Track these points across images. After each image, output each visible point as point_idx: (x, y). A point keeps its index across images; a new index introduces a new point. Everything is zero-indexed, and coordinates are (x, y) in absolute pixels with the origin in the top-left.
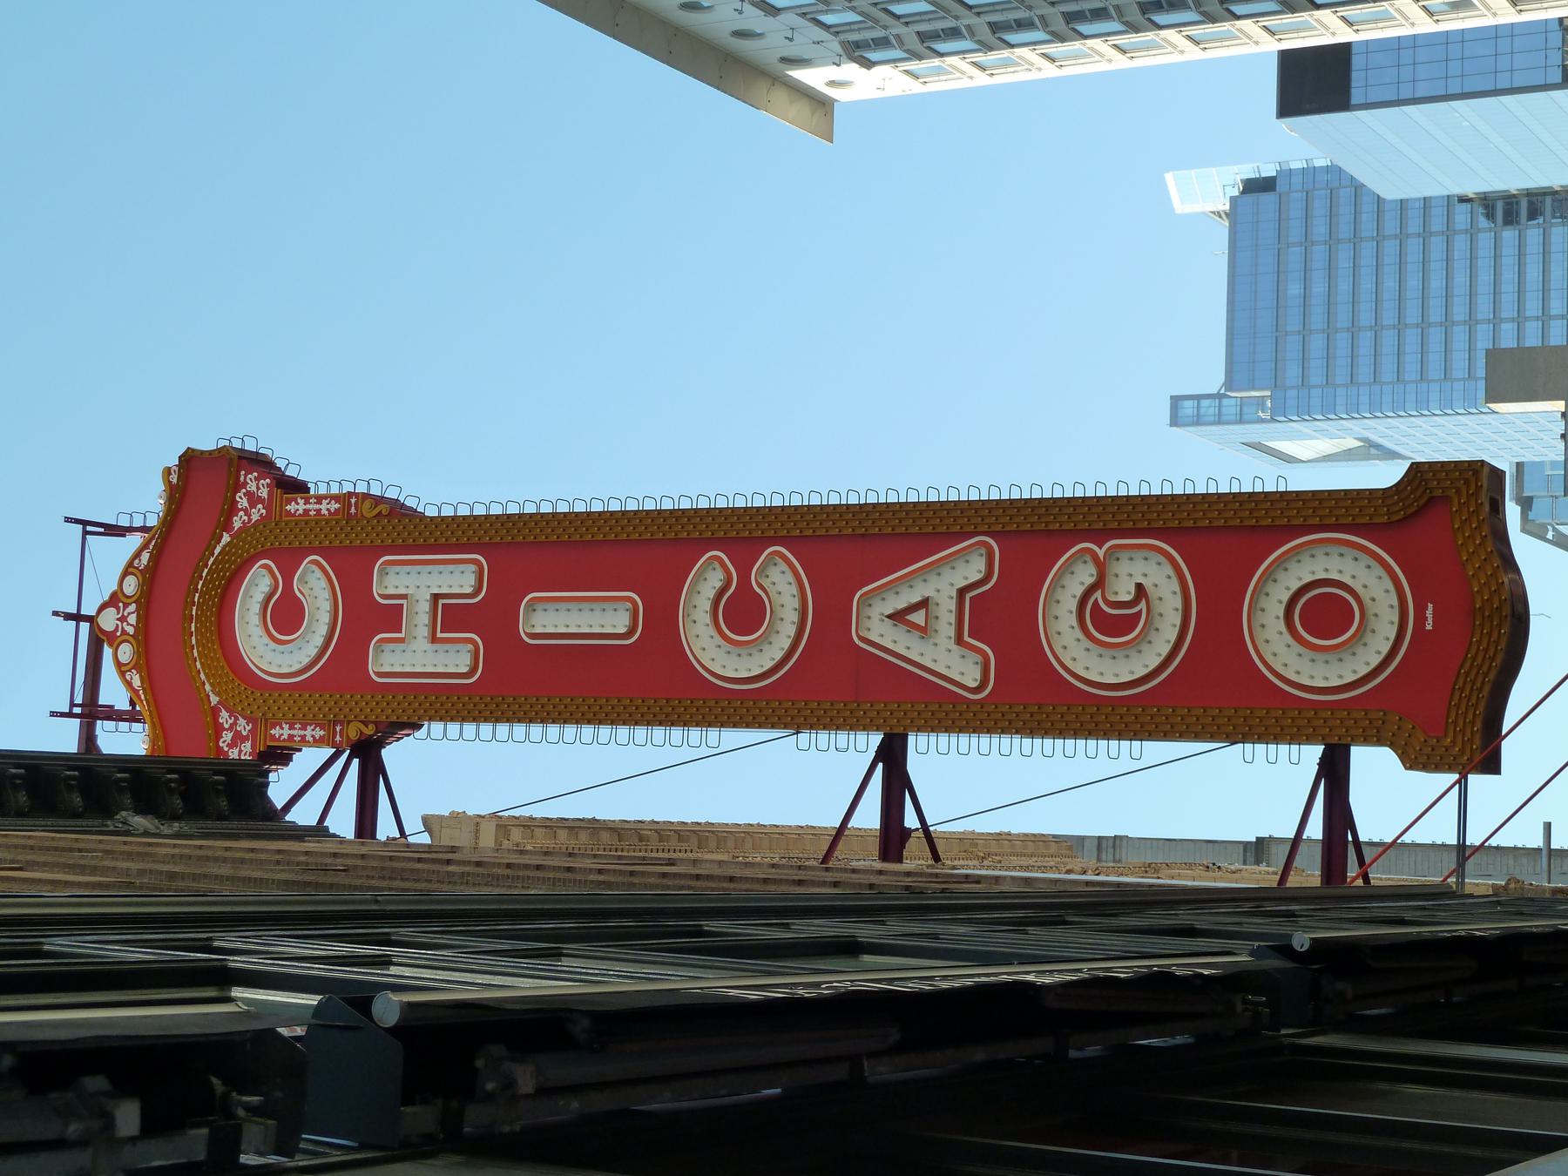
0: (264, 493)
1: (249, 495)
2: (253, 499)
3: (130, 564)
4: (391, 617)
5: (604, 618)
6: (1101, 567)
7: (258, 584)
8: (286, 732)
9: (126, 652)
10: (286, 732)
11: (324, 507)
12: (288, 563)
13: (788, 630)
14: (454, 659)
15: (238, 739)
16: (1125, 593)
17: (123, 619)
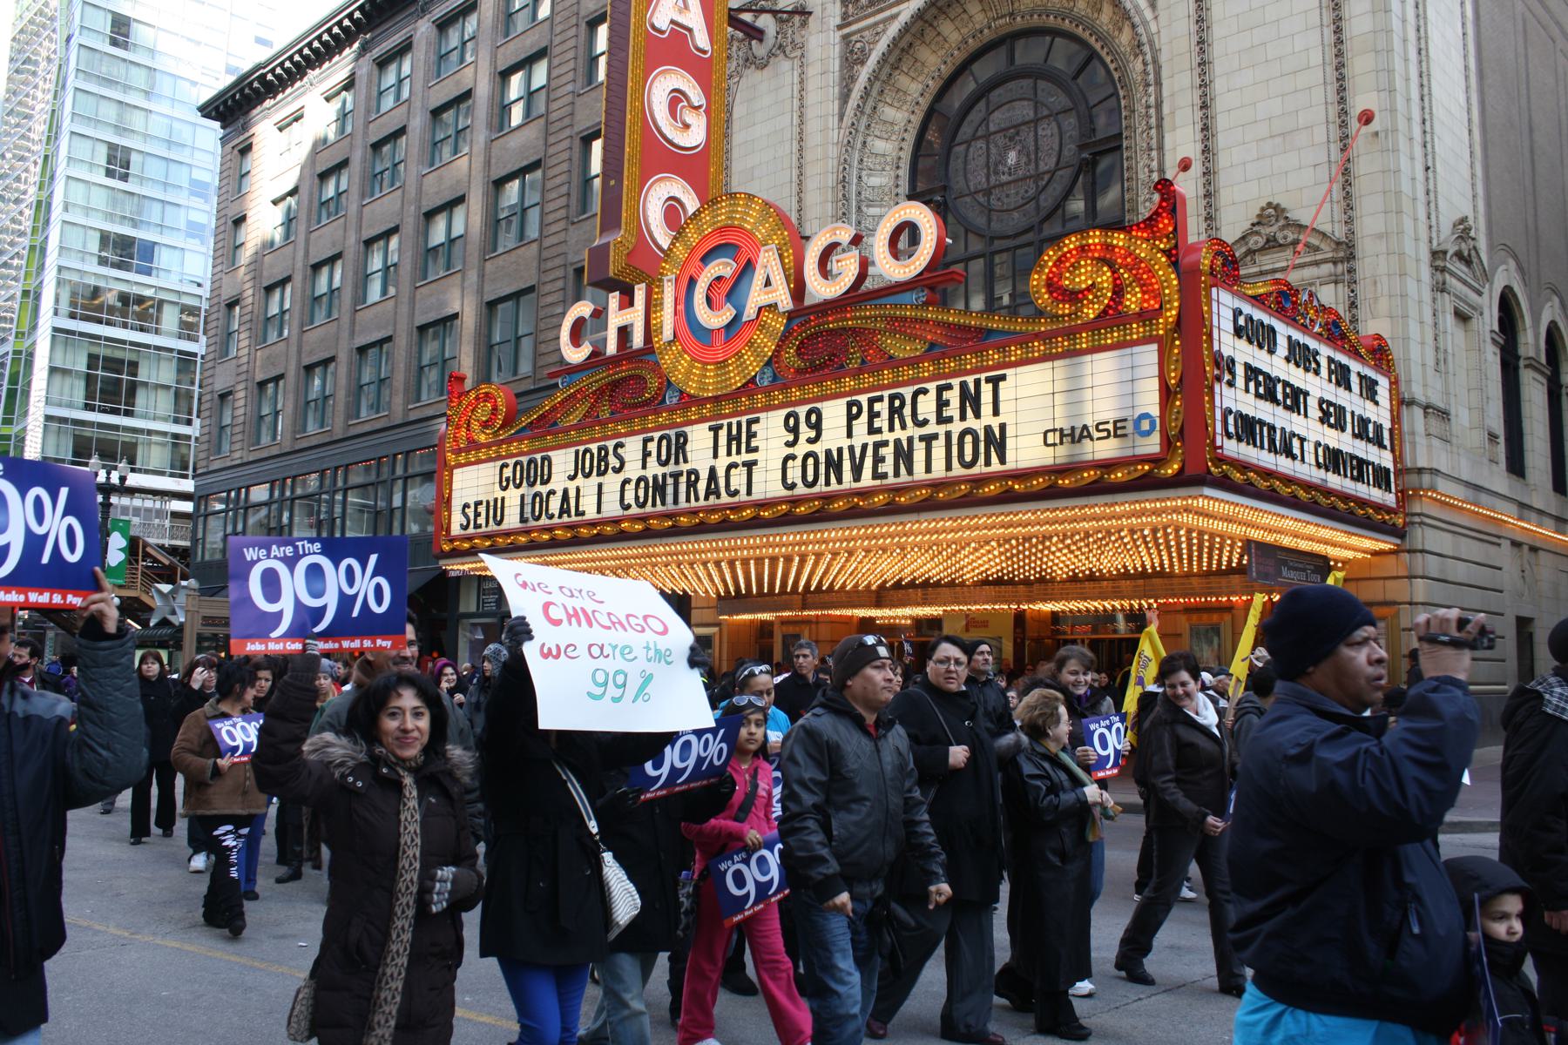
16: (689, 117)
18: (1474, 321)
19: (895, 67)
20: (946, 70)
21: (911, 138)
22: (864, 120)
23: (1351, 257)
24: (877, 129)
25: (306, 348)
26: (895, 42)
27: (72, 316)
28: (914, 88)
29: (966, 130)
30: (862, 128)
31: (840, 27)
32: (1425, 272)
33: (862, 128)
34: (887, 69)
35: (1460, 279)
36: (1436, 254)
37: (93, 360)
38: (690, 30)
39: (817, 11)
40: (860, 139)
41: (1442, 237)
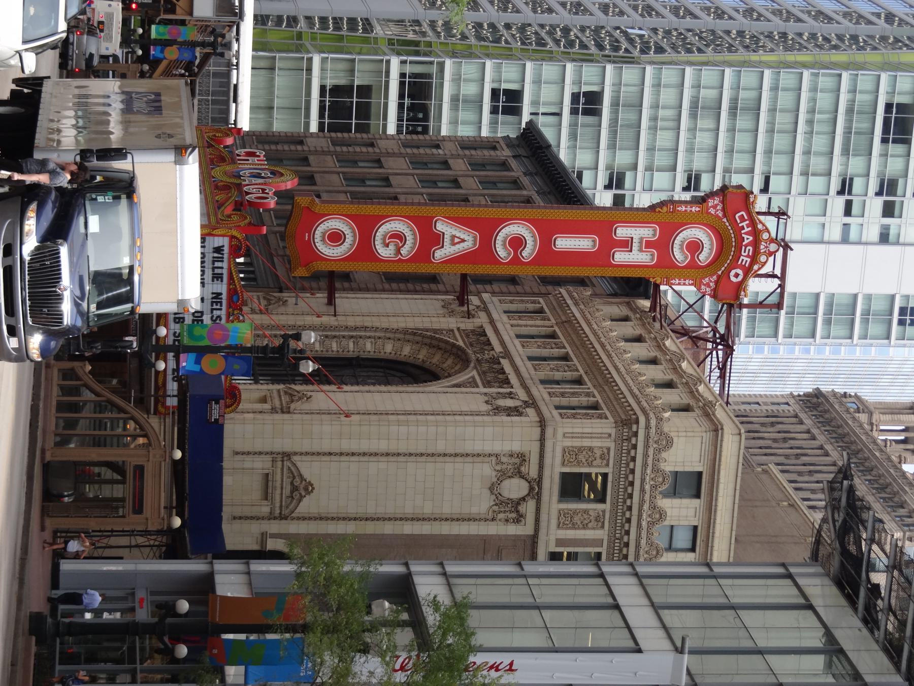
0: (703, 287)
1: (709, 286)
2: (708, 285)
3: (763, 266)
4: (649, 244)
5: (564, 243)
6: (398, 251)
7: (705, 257)
8: (693, 209)
9: (765, 236)
10: (693, 209)
11: (677, 281)
12: (693, 265)
13: (500, 238)
14: (622, 232)
15: (715, 207)
17: (766, 247)
18: (265, 502)
19: (431, 346)
20: (427, 365)
21: (392, 357)
22: (401, 336)
23: (283, 412)
24: (398, 344)
25: (326, 176)
26: (441, 340)
27: (403, 75)
28: (421, 357)
29: (392, 372)
30: (397, 336)
31: (458, 329)
32: (280, 445)
33: (397, 336)
34: (427, 341)
35: (282, 481)
36: (287, 456)
37: (365, 91)
38: (443, 247)
39: (471, 320)
40: (392, 335)
41: (299, 464)
